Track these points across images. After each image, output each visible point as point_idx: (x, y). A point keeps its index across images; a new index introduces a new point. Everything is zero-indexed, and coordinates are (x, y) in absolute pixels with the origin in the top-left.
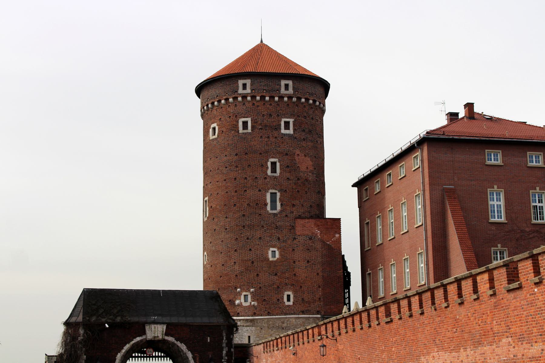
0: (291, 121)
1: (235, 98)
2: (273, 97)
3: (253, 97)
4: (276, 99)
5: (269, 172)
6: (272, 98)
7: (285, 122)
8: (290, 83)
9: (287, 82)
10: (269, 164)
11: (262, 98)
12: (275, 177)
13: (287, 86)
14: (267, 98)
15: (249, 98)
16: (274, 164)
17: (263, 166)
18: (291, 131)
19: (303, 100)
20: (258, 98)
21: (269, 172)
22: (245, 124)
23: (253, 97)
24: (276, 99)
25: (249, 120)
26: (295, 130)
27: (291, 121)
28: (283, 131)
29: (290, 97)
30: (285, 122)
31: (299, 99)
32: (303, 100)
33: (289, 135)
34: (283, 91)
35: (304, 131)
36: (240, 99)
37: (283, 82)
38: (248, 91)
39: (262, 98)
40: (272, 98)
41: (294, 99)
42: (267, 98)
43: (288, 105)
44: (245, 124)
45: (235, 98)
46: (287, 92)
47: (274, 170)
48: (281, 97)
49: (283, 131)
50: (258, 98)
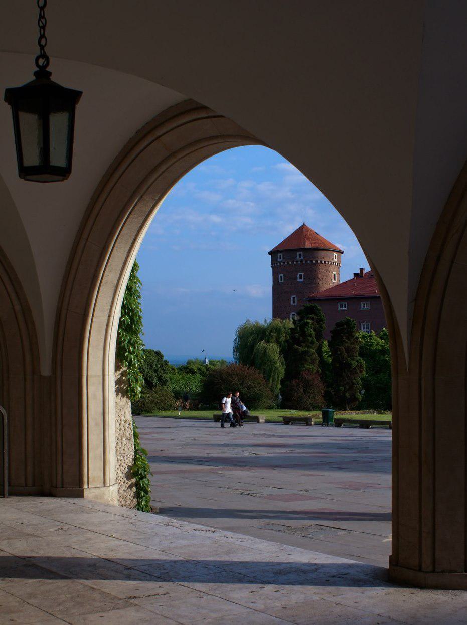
0: (303, 274)
1: (277, 264)
2: (293, 262)
3: (284, 263)
4: (295, 263)
5: (292, 303)
6: (293, 262)
7: (300, 275)
8: (302, 253)
9: (300, 253)
10: (292, 299)
11: (288, 263)
12: (295, 306)
13: (300, 255)
14: (290, 263)
15: (282, 264)
16: (294, 298)
17: (289, 300)
18: (302, 280)
19: (309, 262)
20: (286, 263)
21: (292, 303)
22: (281, 277)
23: (284, 263)
24: (295, 263)
25: (283, 275)
26: (305, 279)
27: (303, 274)
28: (299, 280)
29: (302, 261)
30: (300, 275)
31: (306, 261)
32: (309, 262)
33: (301, 282)
34: (298, 258)
35: (309, 279)
36: (278, 264)
37: (298, 253)
38: (282, 260)
39: (288, 263)
40: (293, 262)
41: (304, 262)
42: (290, 263)
43: (301, 265)
44: (281, 277)
45: (277, 264)
46: (301, 259)
47: (294, 302)
48: (297, 262)
49: (299, 280)
50: (286, 263)
